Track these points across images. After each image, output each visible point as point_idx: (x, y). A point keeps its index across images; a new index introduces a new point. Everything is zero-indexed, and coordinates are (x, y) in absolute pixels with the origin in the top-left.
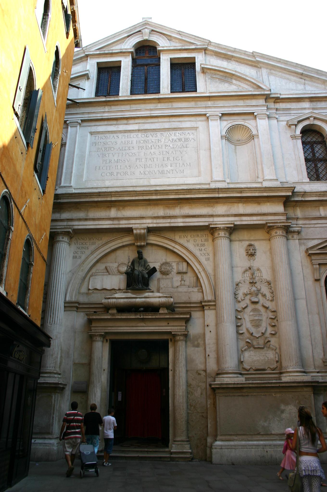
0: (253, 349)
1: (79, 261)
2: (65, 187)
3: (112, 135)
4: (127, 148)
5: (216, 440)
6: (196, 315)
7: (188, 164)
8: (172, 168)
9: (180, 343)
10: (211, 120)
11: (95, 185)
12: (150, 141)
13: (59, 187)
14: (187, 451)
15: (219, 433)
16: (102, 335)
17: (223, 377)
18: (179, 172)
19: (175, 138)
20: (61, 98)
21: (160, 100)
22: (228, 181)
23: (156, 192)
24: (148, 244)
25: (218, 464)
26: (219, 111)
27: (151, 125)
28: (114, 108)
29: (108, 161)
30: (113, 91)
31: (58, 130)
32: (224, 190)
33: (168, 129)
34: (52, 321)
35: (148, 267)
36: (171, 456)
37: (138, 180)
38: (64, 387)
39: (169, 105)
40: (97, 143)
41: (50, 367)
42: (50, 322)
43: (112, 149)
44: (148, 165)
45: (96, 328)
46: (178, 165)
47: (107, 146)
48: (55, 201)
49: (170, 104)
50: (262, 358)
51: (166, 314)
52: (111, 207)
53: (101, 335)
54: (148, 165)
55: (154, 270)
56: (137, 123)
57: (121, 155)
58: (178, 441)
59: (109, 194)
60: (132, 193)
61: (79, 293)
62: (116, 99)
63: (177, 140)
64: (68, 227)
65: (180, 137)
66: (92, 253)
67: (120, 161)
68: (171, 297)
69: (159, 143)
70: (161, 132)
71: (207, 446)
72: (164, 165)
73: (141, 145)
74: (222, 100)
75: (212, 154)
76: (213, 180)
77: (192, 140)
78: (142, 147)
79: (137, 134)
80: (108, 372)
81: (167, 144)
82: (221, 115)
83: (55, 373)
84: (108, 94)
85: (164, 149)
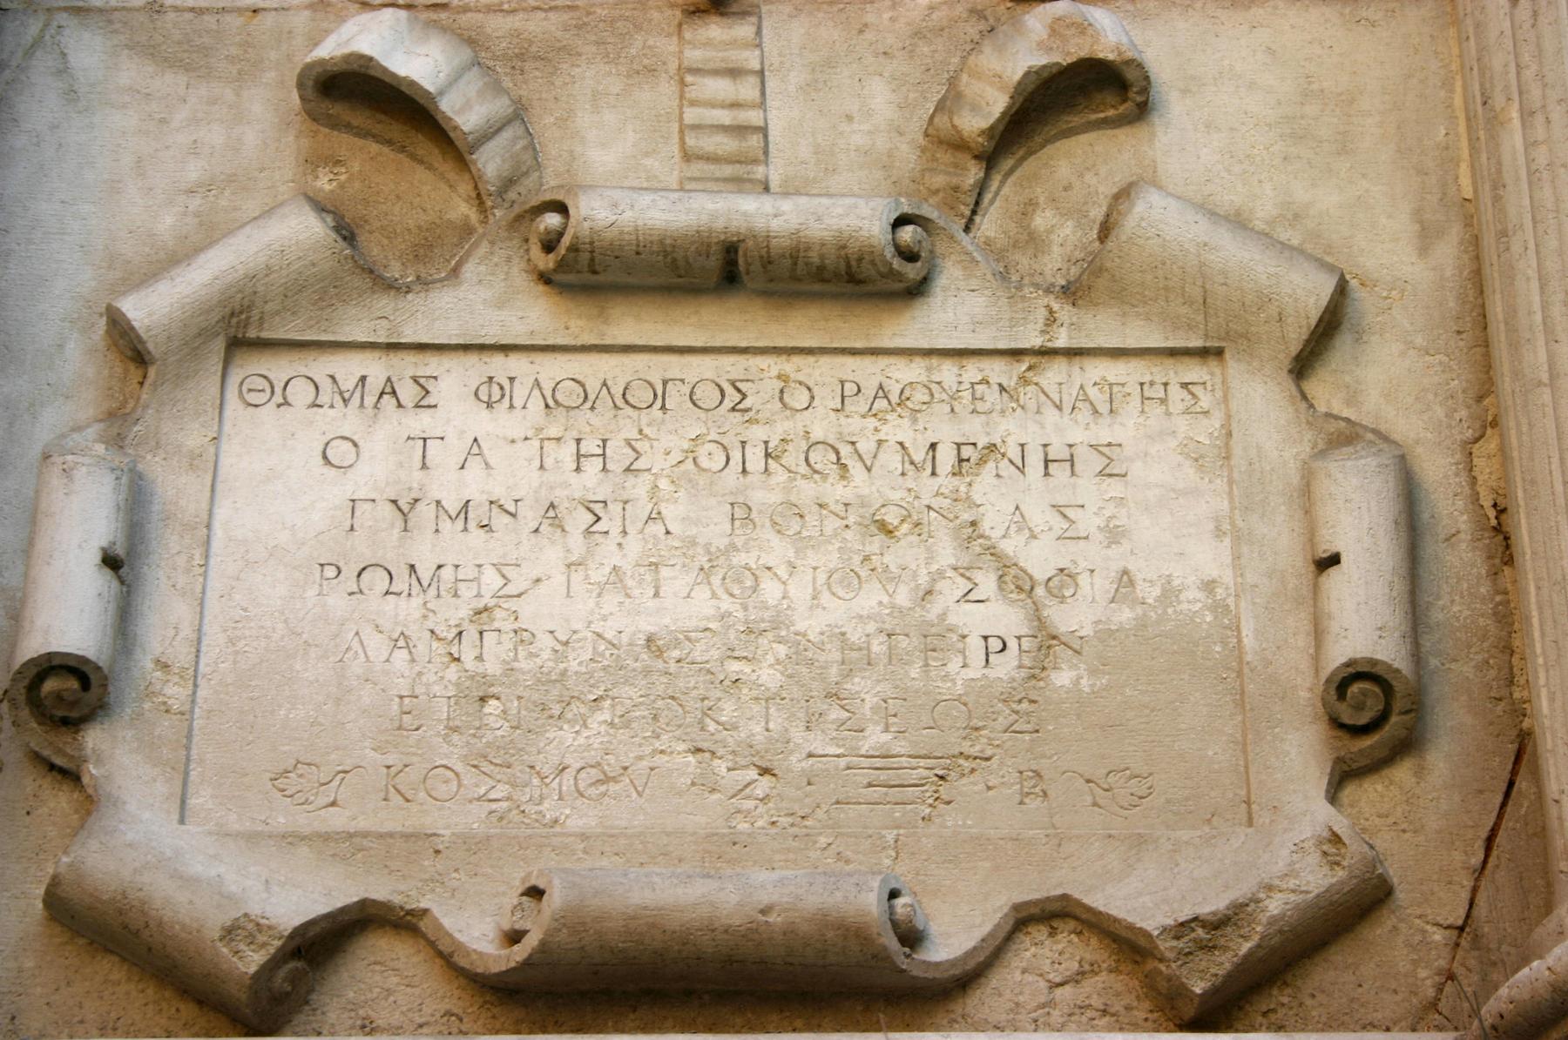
0: (535, 315)
50: (819, 597)
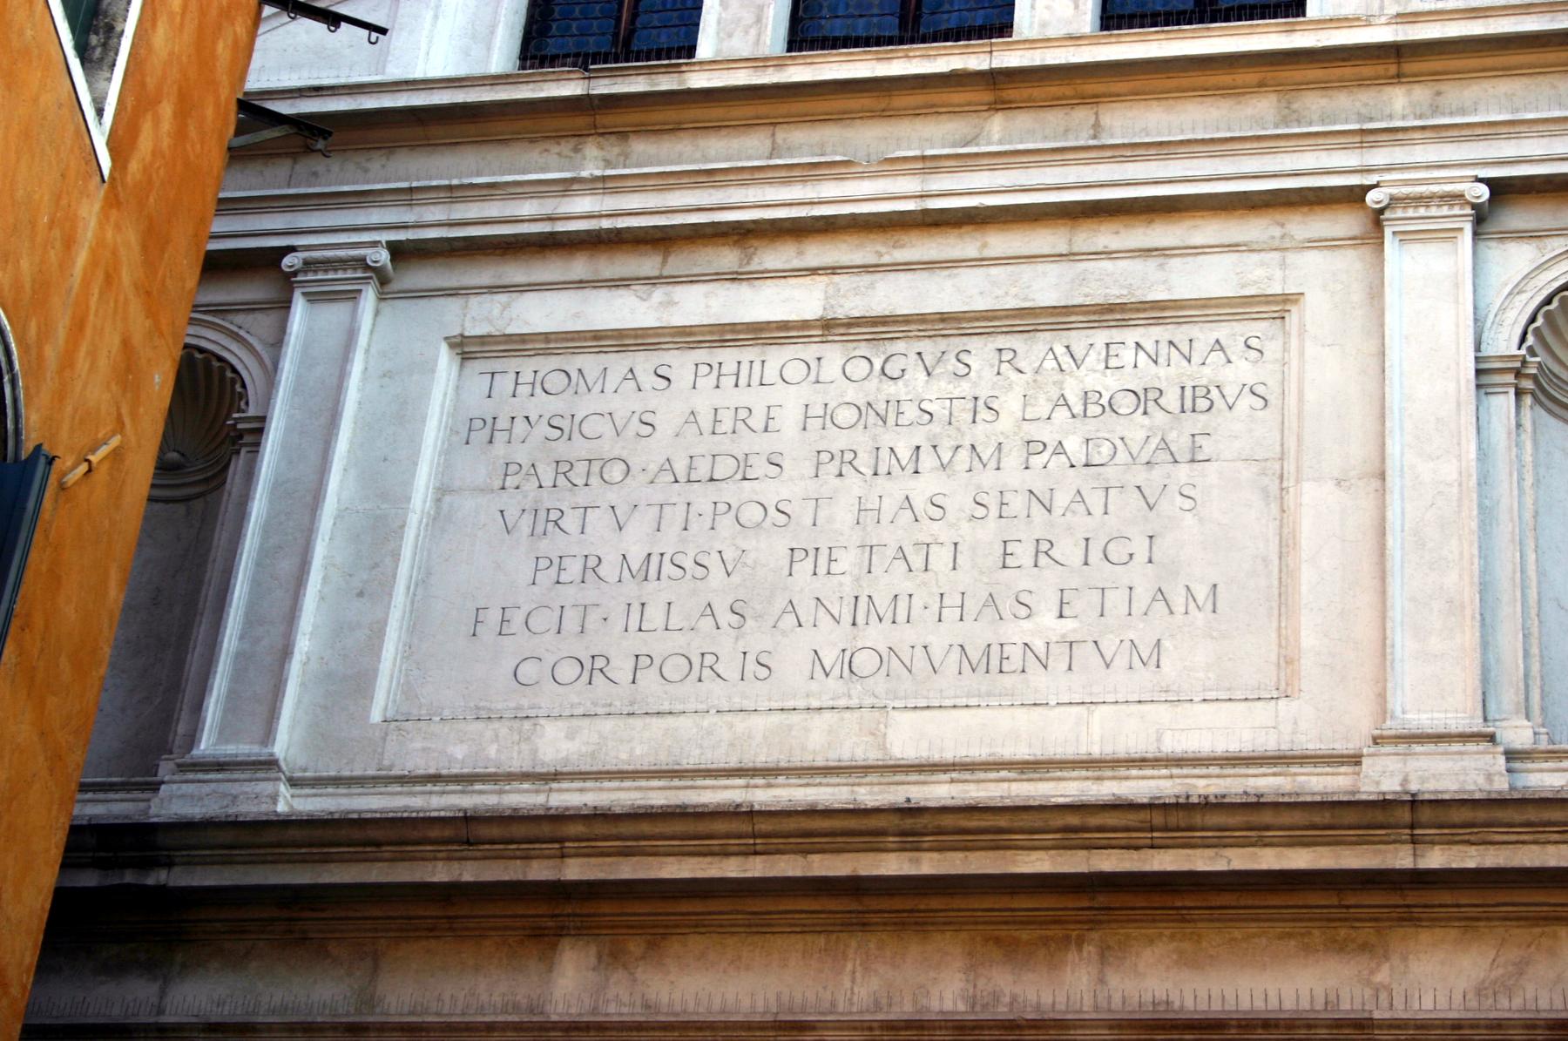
2: (220, 766)
3: (618, 364)
4: (725, 467)
7: (1201, 593)
8: (1068, 625)
10: (1405, 237)
11: (458, 754)
12: (911, 413)
13: (182, 768)
18: (1120, 662)
19: (1109, 384)
20: (167, 110)
21: (1002, 88)
22: (1518, 734)
23: (913, 826)
26: (1464, 167)
27: (920, 279)
28: (652, 155)
29: (574, 569)
30: (655, 20)
31: (126, 343)
32: (1466, 815)
33: (1060, 317)
37: (795, 718)
39: (1071, 125)
40: (503, 423)
43: (616, 472)
44: (883, 604)
46: (1116, 599)
47: (579, 448)
48: (89, 879)
49: (1083, 116)
52: (560, 933)
54: (883, 604)
56: (814, 271)
57: (675, 516)
59: (546, 829)
60: (720, 826)
62: (666, 83)
63: (1126, 403)
65: (1150, 374)
67: (668, 569)
69: (980, 427)
70: (1002, 341)
72: (1007, 605)
73: (838, 441)
74: (1507, 72)
75: (1393, 514)
76: (1392, 727)
77: (1248, 400)
78: (846, 461)
79: (810, 352)
81: (1047, 434)
82: (1483, 192)
84: (625, 49)
85: (1013, 474)
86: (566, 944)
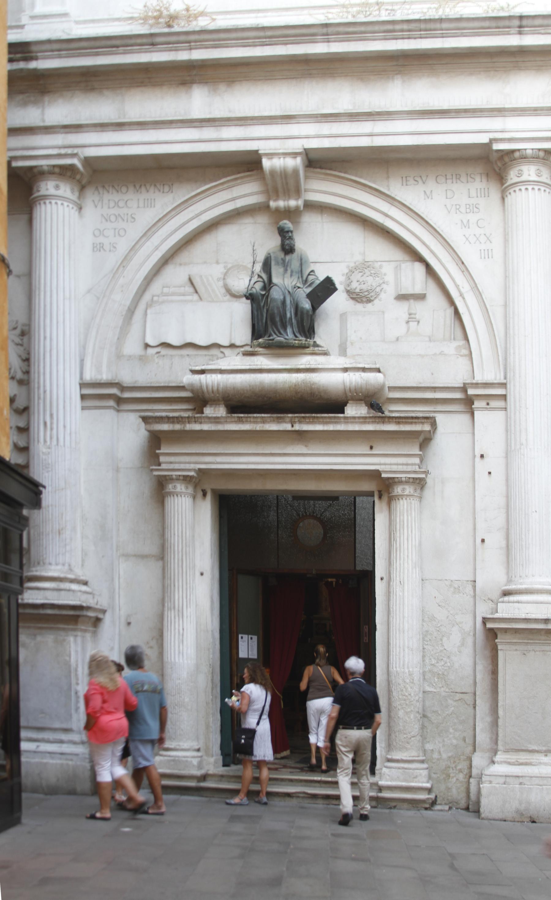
1: (112, 260)
2: (45, 16)
5: (493, 762)
6: (450, 427)
9: (402, 505)
14: (420, 785)
15: (500, 747)
16: (191, 477)
17: (518, 602)
24: (310, 206)
25: (494, 820)
34: (51, 438)
35: (311, 278)
36: (380, 795)
38: (100, 616)
41: (57, 564)
42: (45, 441)
45: (172, 459)
51: (364, 420)
52: (192, 82)
53: (187, 479)
55: (327, 288)
58: (397, 761)
61: (119, 356)
64: (69, 151)
66: (148, 234)
68: (378, 370)
71: (470, 776)
80: (212, 579)
83: (72, 581)
86: (195, 86)
